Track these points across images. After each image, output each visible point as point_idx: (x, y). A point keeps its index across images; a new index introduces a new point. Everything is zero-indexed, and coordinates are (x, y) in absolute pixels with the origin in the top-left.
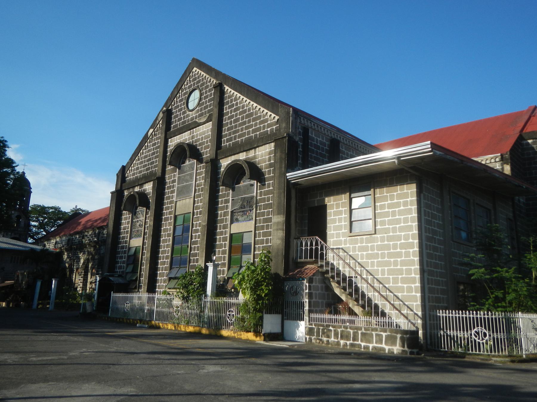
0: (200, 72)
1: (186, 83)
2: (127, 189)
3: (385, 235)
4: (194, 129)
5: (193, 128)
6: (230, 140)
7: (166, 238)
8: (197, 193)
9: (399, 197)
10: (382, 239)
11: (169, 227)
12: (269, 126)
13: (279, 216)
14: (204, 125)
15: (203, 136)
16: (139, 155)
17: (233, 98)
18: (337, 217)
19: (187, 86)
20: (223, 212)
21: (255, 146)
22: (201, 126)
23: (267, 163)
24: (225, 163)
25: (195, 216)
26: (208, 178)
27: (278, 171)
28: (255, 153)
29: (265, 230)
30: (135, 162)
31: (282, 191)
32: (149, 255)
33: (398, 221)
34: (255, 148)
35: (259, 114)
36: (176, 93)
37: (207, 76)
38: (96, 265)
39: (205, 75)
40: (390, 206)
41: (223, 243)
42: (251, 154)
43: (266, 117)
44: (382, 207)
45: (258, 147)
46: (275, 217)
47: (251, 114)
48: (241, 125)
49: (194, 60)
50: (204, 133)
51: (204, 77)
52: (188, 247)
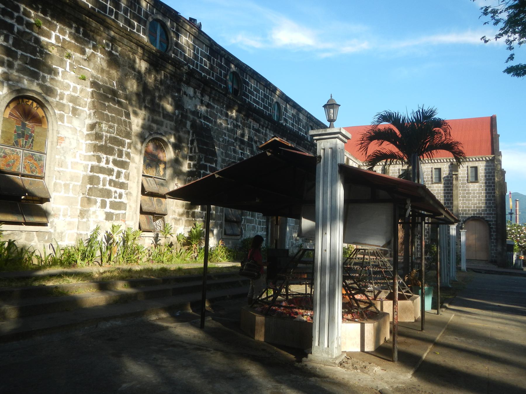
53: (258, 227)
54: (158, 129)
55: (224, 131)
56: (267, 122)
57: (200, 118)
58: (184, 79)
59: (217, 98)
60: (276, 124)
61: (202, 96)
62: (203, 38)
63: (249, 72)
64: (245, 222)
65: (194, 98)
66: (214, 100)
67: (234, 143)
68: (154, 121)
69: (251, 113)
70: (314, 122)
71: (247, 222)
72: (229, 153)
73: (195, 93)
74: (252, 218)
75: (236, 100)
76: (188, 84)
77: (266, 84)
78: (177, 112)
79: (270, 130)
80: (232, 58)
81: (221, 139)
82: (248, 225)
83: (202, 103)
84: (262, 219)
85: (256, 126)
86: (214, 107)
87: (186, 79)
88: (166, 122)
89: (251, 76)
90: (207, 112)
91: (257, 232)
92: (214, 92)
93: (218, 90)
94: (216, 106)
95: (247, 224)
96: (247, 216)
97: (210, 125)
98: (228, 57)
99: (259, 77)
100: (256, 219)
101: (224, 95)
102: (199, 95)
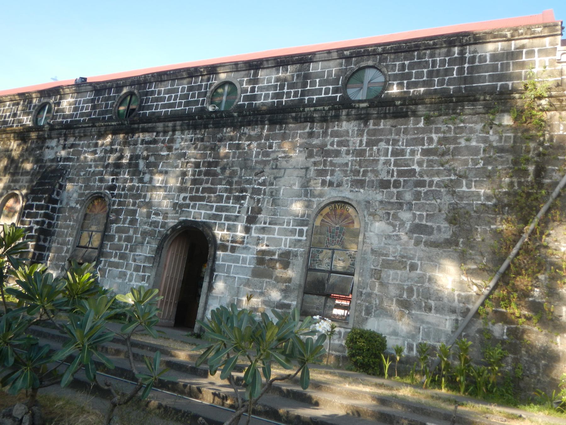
38: (20, 189)
53: (131, 275)
54: (15, 186)
55: (90, 163)
56: (170, 124)
57: (60, 161)
58: (46, 136)
59: (82, 135)
60: (197, 117)
61: (65, 140)
62: (84, 88)
63: (152, 78)
64: (105, 265)
65: (55, 148)
66: (80, 138)
67: (103, 171)
68: (13, 181)
69: (136, 126)
70: (385, 52)
71: (109, 266)
72: (92, 184)
73: (58, 141)
74: (121, 261)
75: (110, 123)
76: (50, 138)
77: (188, 74)
78: (35, 166)
79: (182, 131)
80: (121, 82)
81: (82, 174)
82: (109, 270)
83: (64, 148)
84: (144, 263)
85: (148, 137)
86: (79, 145)
87: (48, 135)
88: (22, 178)
89: (158, 81)
90: (69, 153)
91: (130, 280)
92: (77, 131)
93: (84, 126)
94: (81, 143)
95: (109, 268)
96: (111, 257)
97: (71, 164)
98: (117, 84)
99: (170, 74)
100: (130, 262)
101: (93, 126)
102: (62, 142)
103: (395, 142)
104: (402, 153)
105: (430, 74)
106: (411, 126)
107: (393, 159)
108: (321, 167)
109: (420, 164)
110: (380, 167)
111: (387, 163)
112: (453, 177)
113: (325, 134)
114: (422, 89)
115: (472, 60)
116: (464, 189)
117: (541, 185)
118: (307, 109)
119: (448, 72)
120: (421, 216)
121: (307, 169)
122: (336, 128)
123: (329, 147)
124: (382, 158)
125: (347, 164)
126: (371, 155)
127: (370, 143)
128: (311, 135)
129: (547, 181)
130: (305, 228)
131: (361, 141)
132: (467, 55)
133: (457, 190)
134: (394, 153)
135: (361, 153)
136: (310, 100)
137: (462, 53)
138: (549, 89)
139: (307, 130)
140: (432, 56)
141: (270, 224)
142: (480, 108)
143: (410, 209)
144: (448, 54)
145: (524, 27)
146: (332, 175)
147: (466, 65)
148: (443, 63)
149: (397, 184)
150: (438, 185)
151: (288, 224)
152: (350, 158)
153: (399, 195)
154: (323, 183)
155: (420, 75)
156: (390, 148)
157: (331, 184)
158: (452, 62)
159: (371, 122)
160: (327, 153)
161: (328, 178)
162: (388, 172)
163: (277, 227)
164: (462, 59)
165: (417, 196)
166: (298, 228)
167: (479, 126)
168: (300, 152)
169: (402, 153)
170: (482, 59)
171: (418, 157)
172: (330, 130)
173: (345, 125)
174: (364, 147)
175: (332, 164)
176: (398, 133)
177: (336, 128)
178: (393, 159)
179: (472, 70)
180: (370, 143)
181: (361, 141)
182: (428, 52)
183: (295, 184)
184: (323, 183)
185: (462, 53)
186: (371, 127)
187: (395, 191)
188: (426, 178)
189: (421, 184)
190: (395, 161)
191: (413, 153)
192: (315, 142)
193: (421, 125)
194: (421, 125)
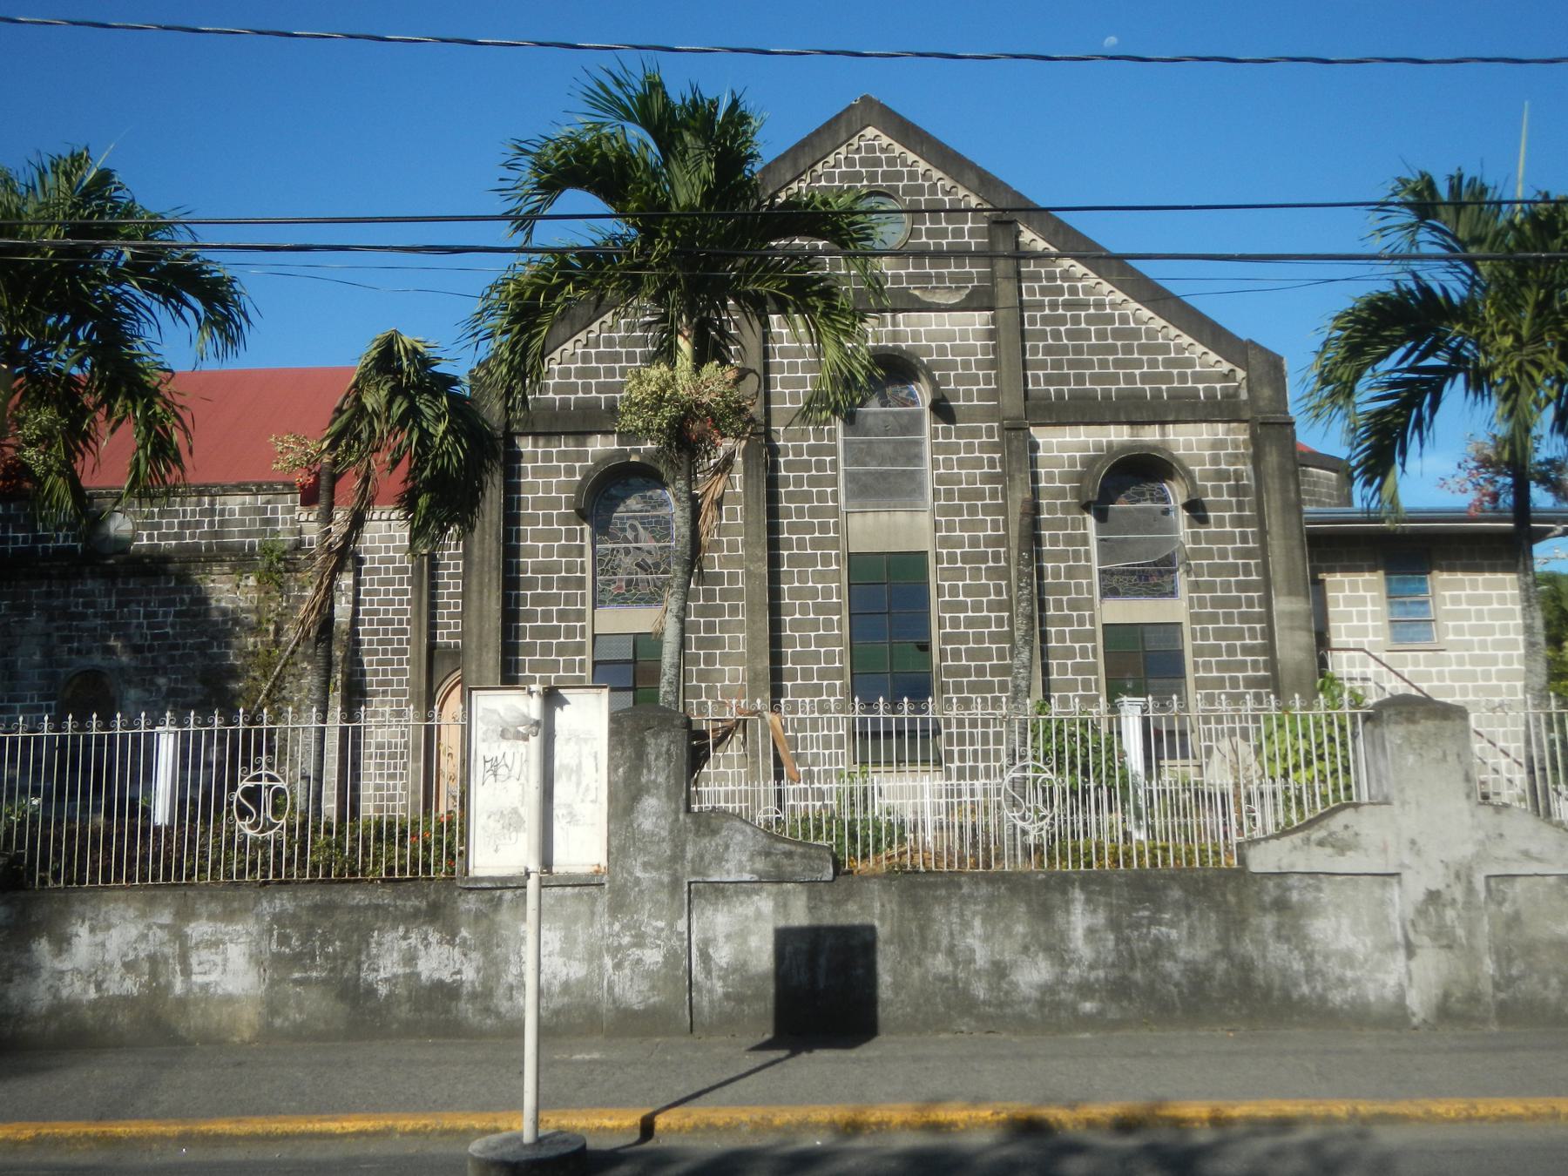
0: (898, 148)
1: (831, 159)
2: (536, 435)
3: (1466, 653)
4: (900, 316)
5: (895, 311)
6: (1064, 380)
7: (812, 616)
8: (942, 502)
9: (1488, 585)
10: (1461, 661)
11: (819, 586)
12: (1198, 378)
13: (1294, 599)
14: (946, 314)
15: (948, 344)
16: (595, 326)
17: (1058, 270)
18: (1354, 609)
19: (837, 171)
20: (1062, 565)
21: (1171, 419)
22: (933, 314)
23: (1208, 467)
24: (1054, 440)
25: (945, 565)
26: (1020, 471)
27: (1278, 496)
28: (1163, 434)
29: (1222, 625)
30: (569, 345)
31: (1296, 542)
32: (767, 663)
33: (1490, 630)
34: (1163, 423)
35: (1160, 341)
36: (789, 177)
37: (936, 174)
39: (922, 166)
40: (1471, 600)
41: (1077, 646)
42: (1151, 435)
43: (1187, 355)
44: (1456, 600)
45: (1175, 422)
46: (1282, 599)
47: (1135, 334)
48: (1093, 350)
49: (866, 100)
50: (950, 336)
51: (921, 171)
52: (925, 648)
103: (147, 604)
104: (155, 614)
105: (182, 525)
106: (162, 585)
107: (145, 622)
108: (66, 633)
109: (173, 626)
110: (132, 630)
111: (139, 626)
112: (204, 639)
113: (67, 594)
114: (174, 542)
115: (222, 512)
116: (215, 650)
117: (277, 643)
118: (42, 564)
119: (199, 524)
120: (176, 680)
121: (49, 635)
122: (79, 587)
123: (73, 609)
124: (135, 621)
125: (95, 629)
126: (121, 618)
127: (120, 605)
128: (49, 594)
129: (284, 639)
130: (53, 703)
131: (110, 603)
132: (217, 507)
133: (209, 651)
134: (146, 616)
135: (110, 616)
136: (45, 549)
137: (212, 503)
138: (284, 553)
139: (44, 589)
140: (182, 504)
141: (9, 701)
142: (226, 569)
143: (165, 674)
144: (199, 504)
145: (267, 483)
146: (79, 641)
147: (217, 518)
148: (193, 513)
149: (151, 648)
150: (191, 647)
151: (32, 699)
152: (99, 622)
153: (154, 660)
154: (70, 651)
155: (170, 525)
156: (142, 610)
157: (79, 652)
158: (203, 512)
159: (120, 580)
160: (73, 617)
161: (76, 644)
162: (141, 636)
163: (18, 705)
164: (212, 512)
165: (172, 659)
166: (44, 703)
167: (228, 586)
168: (38, 615)
169: (155, 614)
170: (232, 512)
171: (171, 619)
172: (72, 590)
173: (90, 584)
174: (113, 608)
175: (78, 629)
176: (149, 593)
177: (79, 587)
178: (145, 622)
179: (222, 523)
180: (120, 605)
181: (110, 603)
182: (178, 499)
183: (35, 654)
184: (70, 651)
185: (212, 503)
186: (120, 586)
187: (150, 655)
188: (180, 641)
189: (175, 647)
190: (148, 624)
191: (166, 615)
192: (56, 603)
193: (173, 584)
194: (173, 584)
